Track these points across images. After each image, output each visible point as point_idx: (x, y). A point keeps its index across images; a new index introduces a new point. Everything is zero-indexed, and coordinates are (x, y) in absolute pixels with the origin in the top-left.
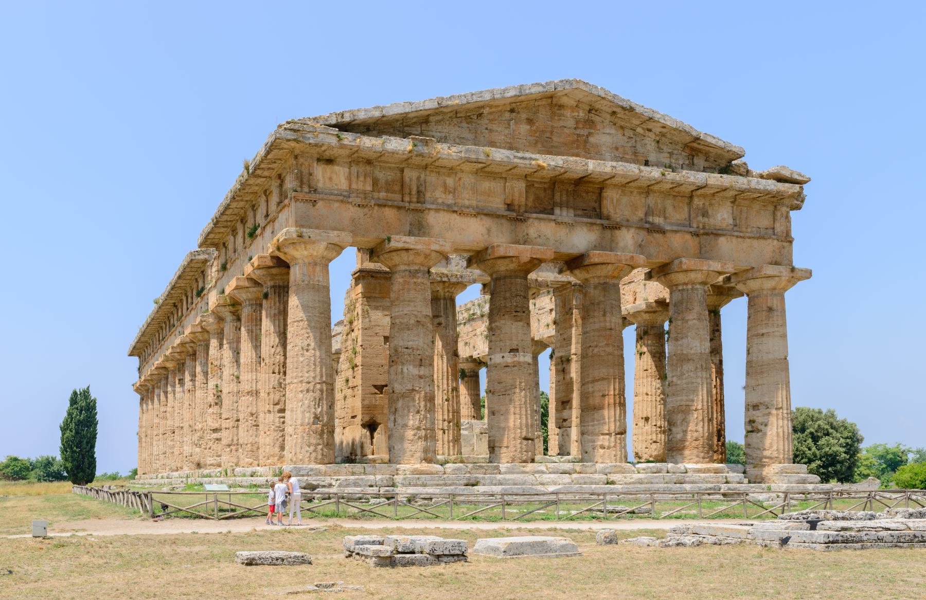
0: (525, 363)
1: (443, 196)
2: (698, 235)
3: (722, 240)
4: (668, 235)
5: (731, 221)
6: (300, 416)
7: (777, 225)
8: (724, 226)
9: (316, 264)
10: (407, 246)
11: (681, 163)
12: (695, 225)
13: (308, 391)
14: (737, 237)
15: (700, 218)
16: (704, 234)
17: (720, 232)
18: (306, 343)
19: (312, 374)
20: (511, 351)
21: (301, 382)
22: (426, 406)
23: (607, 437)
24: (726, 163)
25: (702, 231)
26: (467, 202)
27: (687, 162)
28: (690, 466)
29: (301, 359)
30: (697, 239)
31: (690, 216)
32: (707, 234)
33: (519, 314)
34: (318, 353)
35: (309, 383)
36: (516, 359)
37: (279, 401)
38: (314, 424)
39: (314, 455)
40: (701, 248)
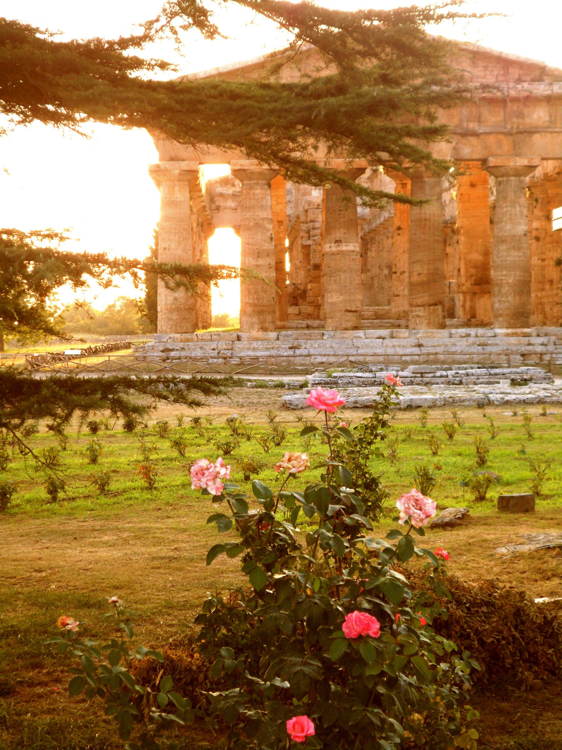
0: (346, 251)
2: (511, 135)
3: (536, 136)
4: (482, 137)
5: (547, 118)
8: (540, 123)
11: (495, 73)
12: (509, 126)
14: (552, 132)
15: (515, 120)
16: (517, 133)
17: (533, 130)
20: (336, 242)
23: (422, 308)
25: (515, 131)
27: (502, 72)
28: (499, 331)
30: (511, 139)
31: (505, 118)
32: (520, 133)
33: (342, 212)
36: (339, 249)
40: (515, 145)
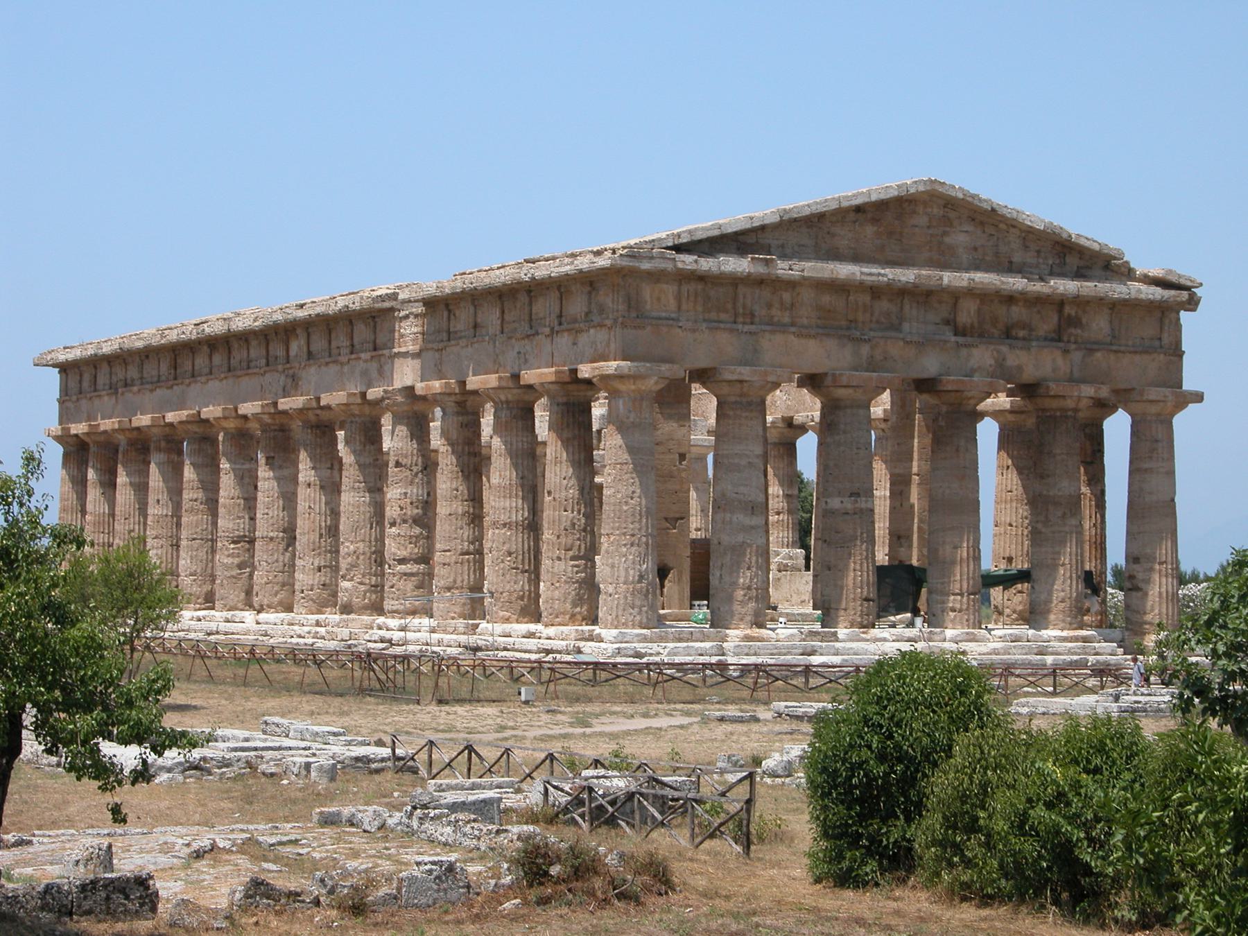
1: (779, 313)
6: (623, 574)
7: (1165, 336)
9: (642, 399)
10: (741, 378)
13: (632, 545)
18: (631, 489)
19: (637, 525)
21: (624, 534)
22: (757, 562)
24: (1106, 264)
26: (805, 321)
29: (625, 508)
34: (644, 502)
35: (633, 535)
37: (572, 545)
38: (640, 581)
39: (638, 618)
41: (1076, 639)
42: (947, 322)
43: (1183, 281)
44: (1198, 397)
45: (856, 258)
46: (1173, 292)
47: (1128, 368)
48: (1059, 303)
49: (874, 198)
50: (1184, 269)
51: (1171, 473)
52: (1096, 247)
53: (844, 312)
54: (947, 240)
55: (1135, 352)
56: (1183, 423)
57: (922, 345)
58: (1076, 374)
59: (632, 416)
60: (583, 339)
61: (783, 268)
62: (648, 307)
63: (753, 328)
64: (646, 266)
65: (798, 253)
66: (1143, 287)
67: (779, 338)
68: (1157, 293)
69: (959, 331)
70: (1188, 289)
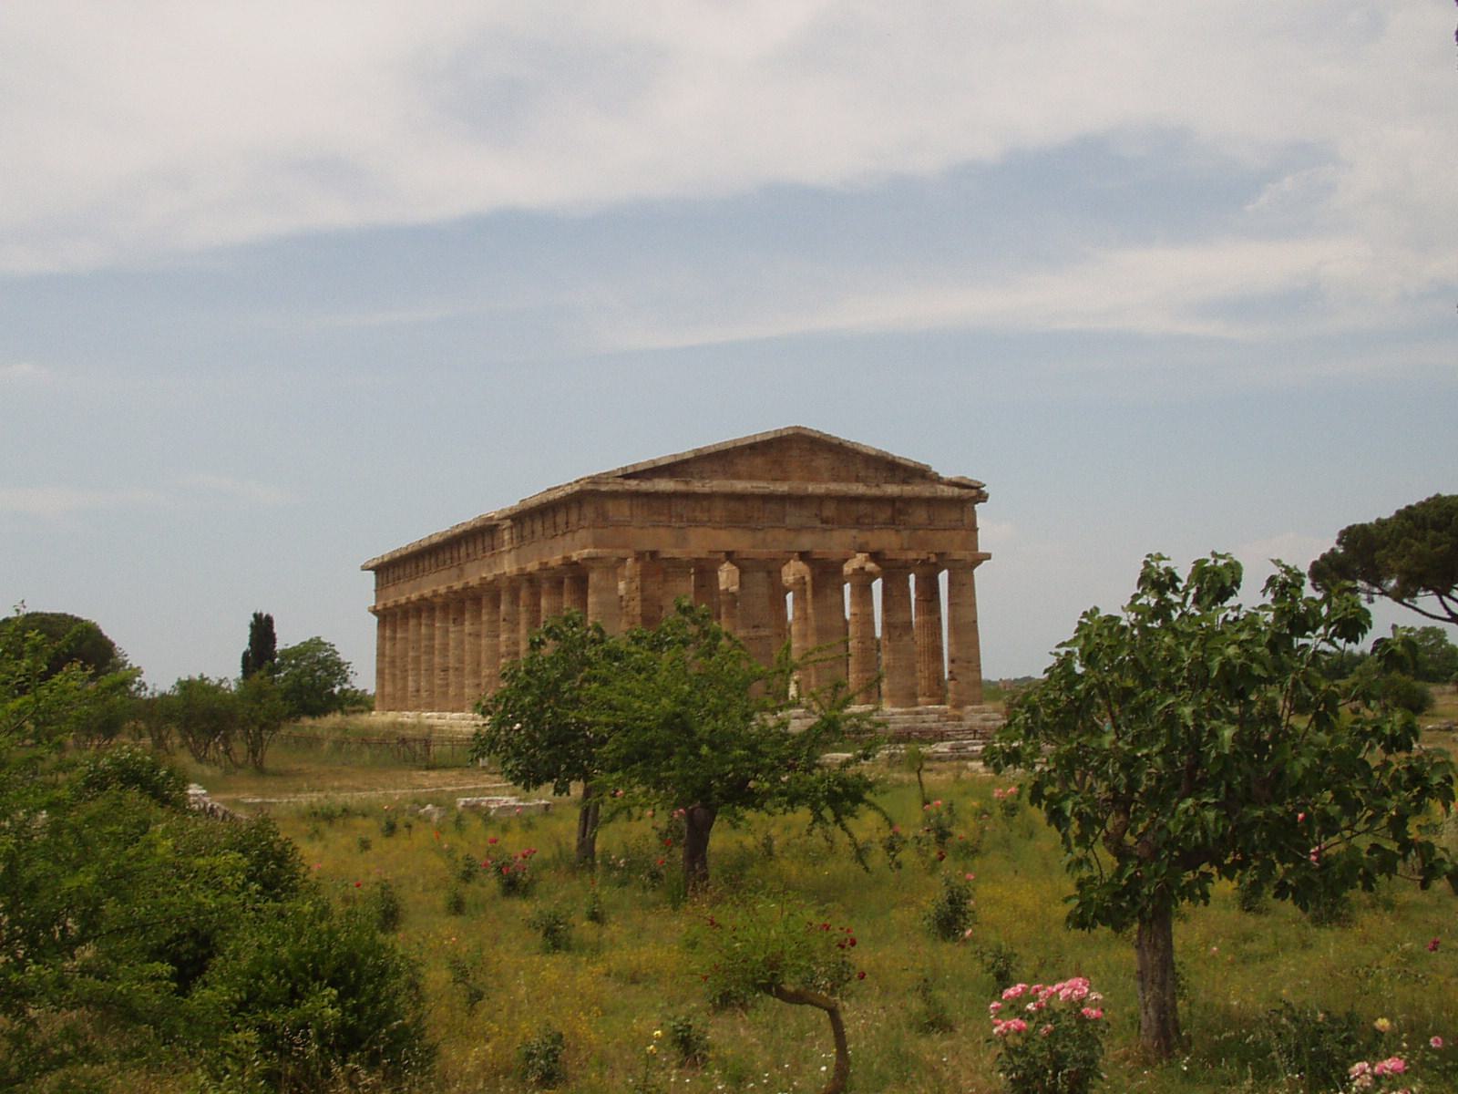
20: (754, 627)
26: (718, 519)
41: (908, 713)
42: (816, 515)
43: (972, 484)
44: (988, 557)
45: (751, 477)
46: (966, 491)
47: (941, 540)
48: (891, 500)
49: (758, 439)
50: (972, 475)
51: (973, 605)
52: (912, 465)
53: (743, 509)
54: (814, 464)
55: (945, 530)
56: (979, 573)
57: (799, 529)
58: (906, 546)
59: (602, 583)
60: (577, 536)
61: (697, 486)
62: (611, 514)
63: (682, 525)
64: (604, 488)
65: (713, 475)
66: (946, 488)
67: (701, 530)
68: (956, 491)
69: (824, 521)
70: (977, 488)
